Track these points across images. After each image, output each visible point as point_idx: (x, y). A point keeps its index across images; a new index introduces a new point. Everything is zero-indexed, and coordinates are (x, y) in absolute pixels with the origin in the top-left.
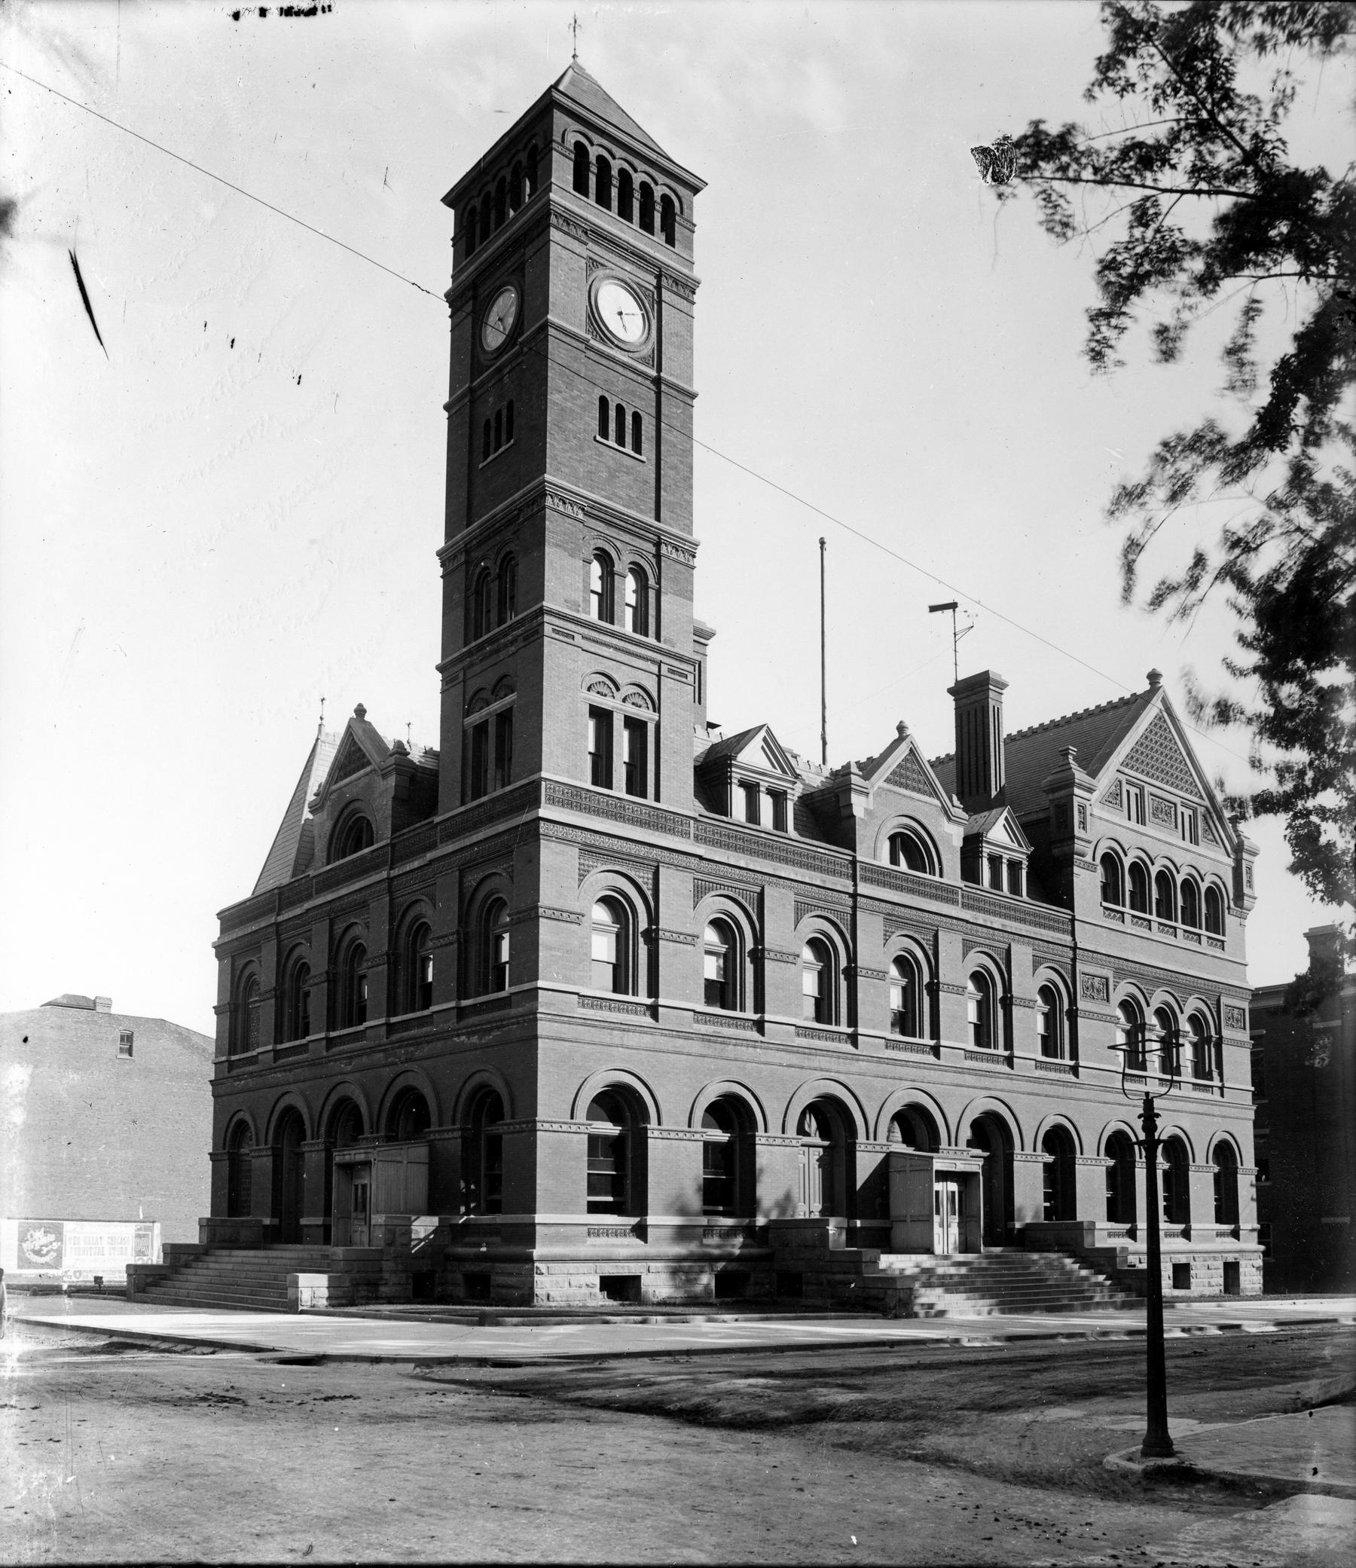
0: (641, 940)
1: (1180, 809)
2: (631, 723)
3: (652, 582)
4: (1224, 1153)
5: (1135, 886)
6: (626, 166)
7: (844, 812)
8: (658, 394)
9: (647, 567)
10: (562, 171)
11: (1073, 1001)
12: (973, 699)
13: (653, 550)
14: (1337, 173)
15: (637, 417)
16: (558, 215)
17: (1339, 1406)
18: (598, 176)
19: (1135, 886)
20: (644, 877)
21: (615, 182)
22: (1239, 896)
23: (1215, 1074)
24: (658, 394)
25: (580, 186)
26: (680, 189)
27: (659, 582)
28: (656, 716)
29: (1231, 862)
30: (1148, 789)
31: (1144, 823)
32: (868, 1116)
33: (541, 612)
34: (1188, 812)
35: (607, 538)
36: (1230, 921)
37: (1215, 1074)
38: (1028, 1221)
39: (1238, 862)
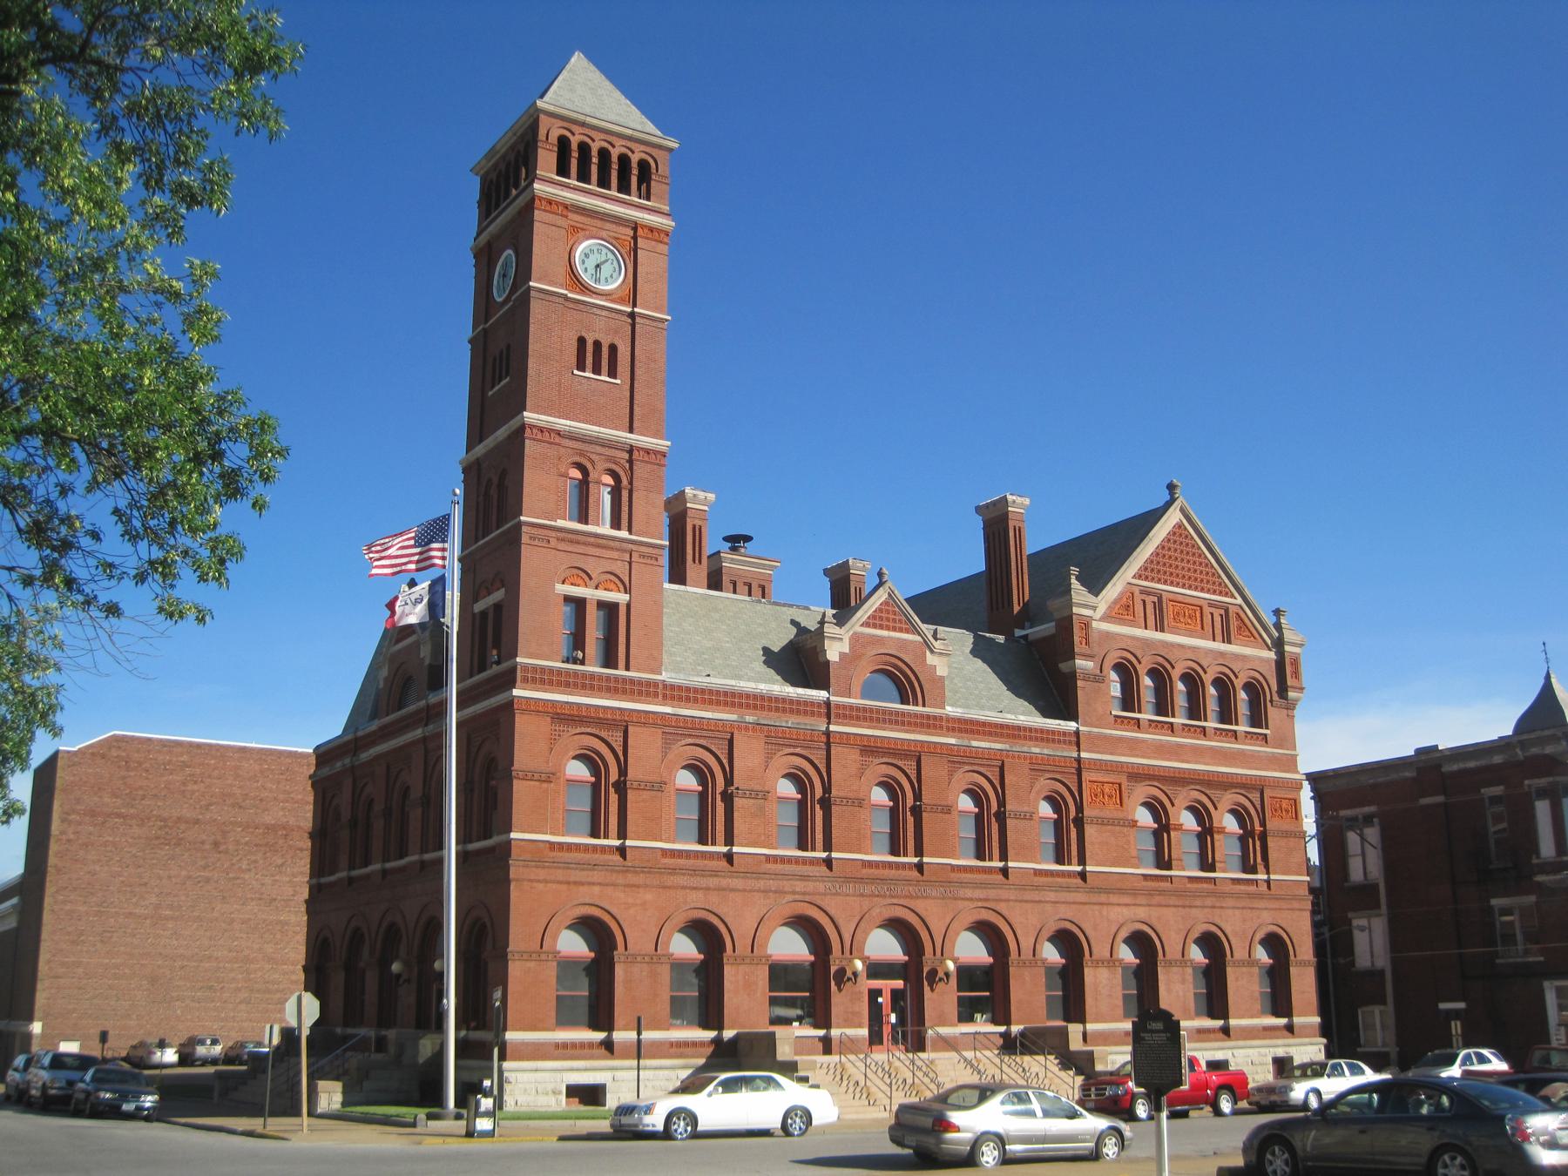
0: (612, 790)
1: (1207, 610)
2: (610, 609)
3: (625, 482)
4: (1275, 944)
5: (1156, 687)
6: (606, 145)
7: (821, 659)
8: (633, 326)
9: (622, 474)
10: (546, 160)
11: (1080, 809)
12: (997, 528)
13: (627, 456)
14: (8, 526)
15: (613, 349)
16: (541, 199)
17: (155, 1124)
18: (579, 160)
19: (1156, 687)
20: (616, 739)
21: (595, 160)
22: (1283, 689)
23: (1261, 867)
24: (633, 326)
25: (563, 170)
26: (654, 152)
27: (631, 483)
28: (627, 597)
29: (1272, 655)
30: (1165, 596)
31: (1162, 630)
32: (843, 930)
33: (520, 524)
34: (1217, 612)
35: (582, 454)
36: (1274, 714)
37: (1261, 867)
38: (1183, 1024)
39: (1281, 654)
